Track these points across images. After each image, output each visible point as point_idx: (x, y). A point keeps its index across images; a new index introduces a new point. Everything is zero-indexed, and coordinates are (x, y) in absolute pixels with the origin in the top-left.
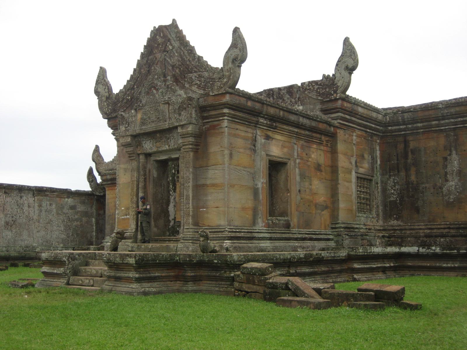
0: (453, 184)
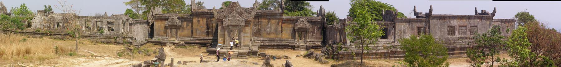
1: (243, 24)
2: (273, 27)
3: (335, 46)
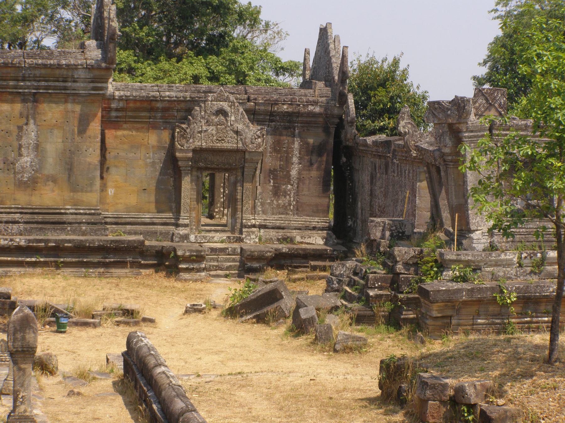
0: (29, 159)
2: (54, 146)
3: (403, 252)
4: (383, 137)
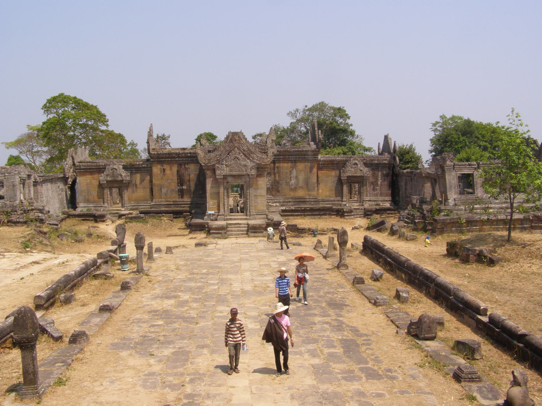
1: (254, 172)
2: (302, 177)
3: (425, 207)
4: (409, 170)
